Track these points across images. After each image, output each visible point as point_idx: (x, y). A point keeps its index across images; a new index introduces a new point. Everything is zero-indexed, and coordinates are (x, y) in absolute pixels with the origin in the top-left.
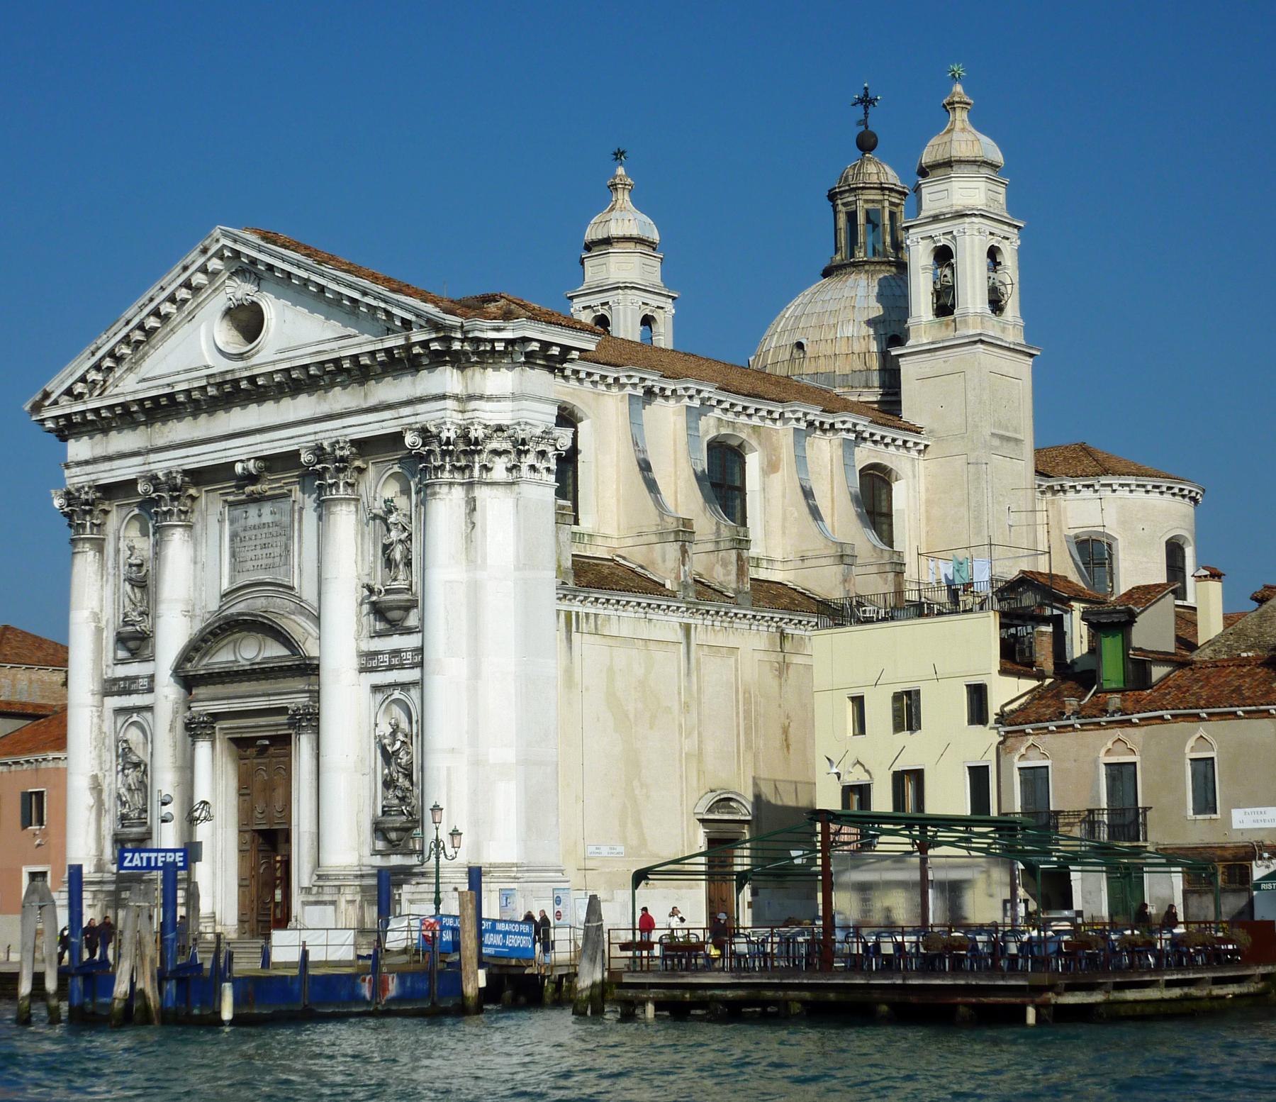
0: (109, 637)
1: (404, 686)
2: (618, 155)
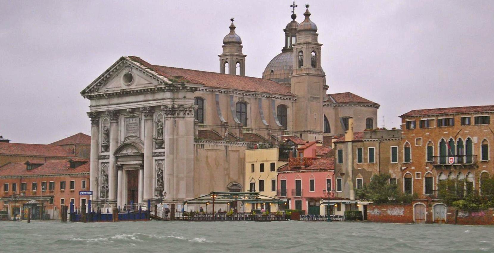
0: (100, 146)
2: (232, 20)
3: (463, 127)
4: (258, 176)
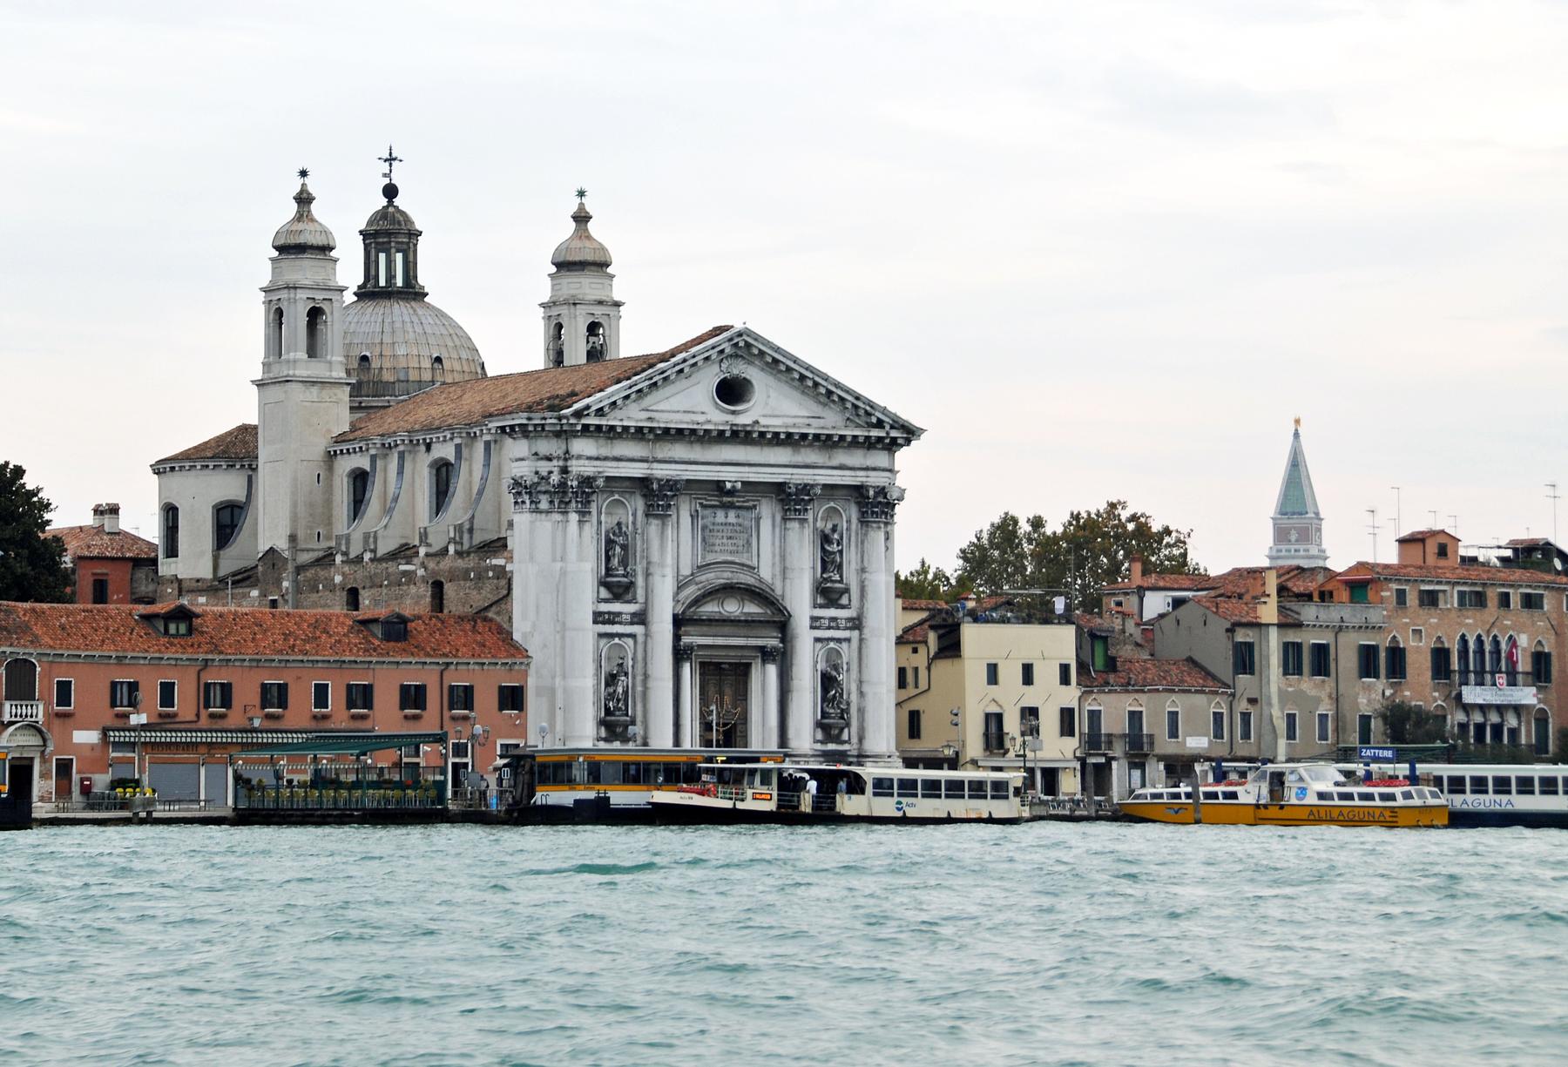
1: (839, 640)
2: (304, 173)
3: (1502, 612)
4: (1010, 697)
